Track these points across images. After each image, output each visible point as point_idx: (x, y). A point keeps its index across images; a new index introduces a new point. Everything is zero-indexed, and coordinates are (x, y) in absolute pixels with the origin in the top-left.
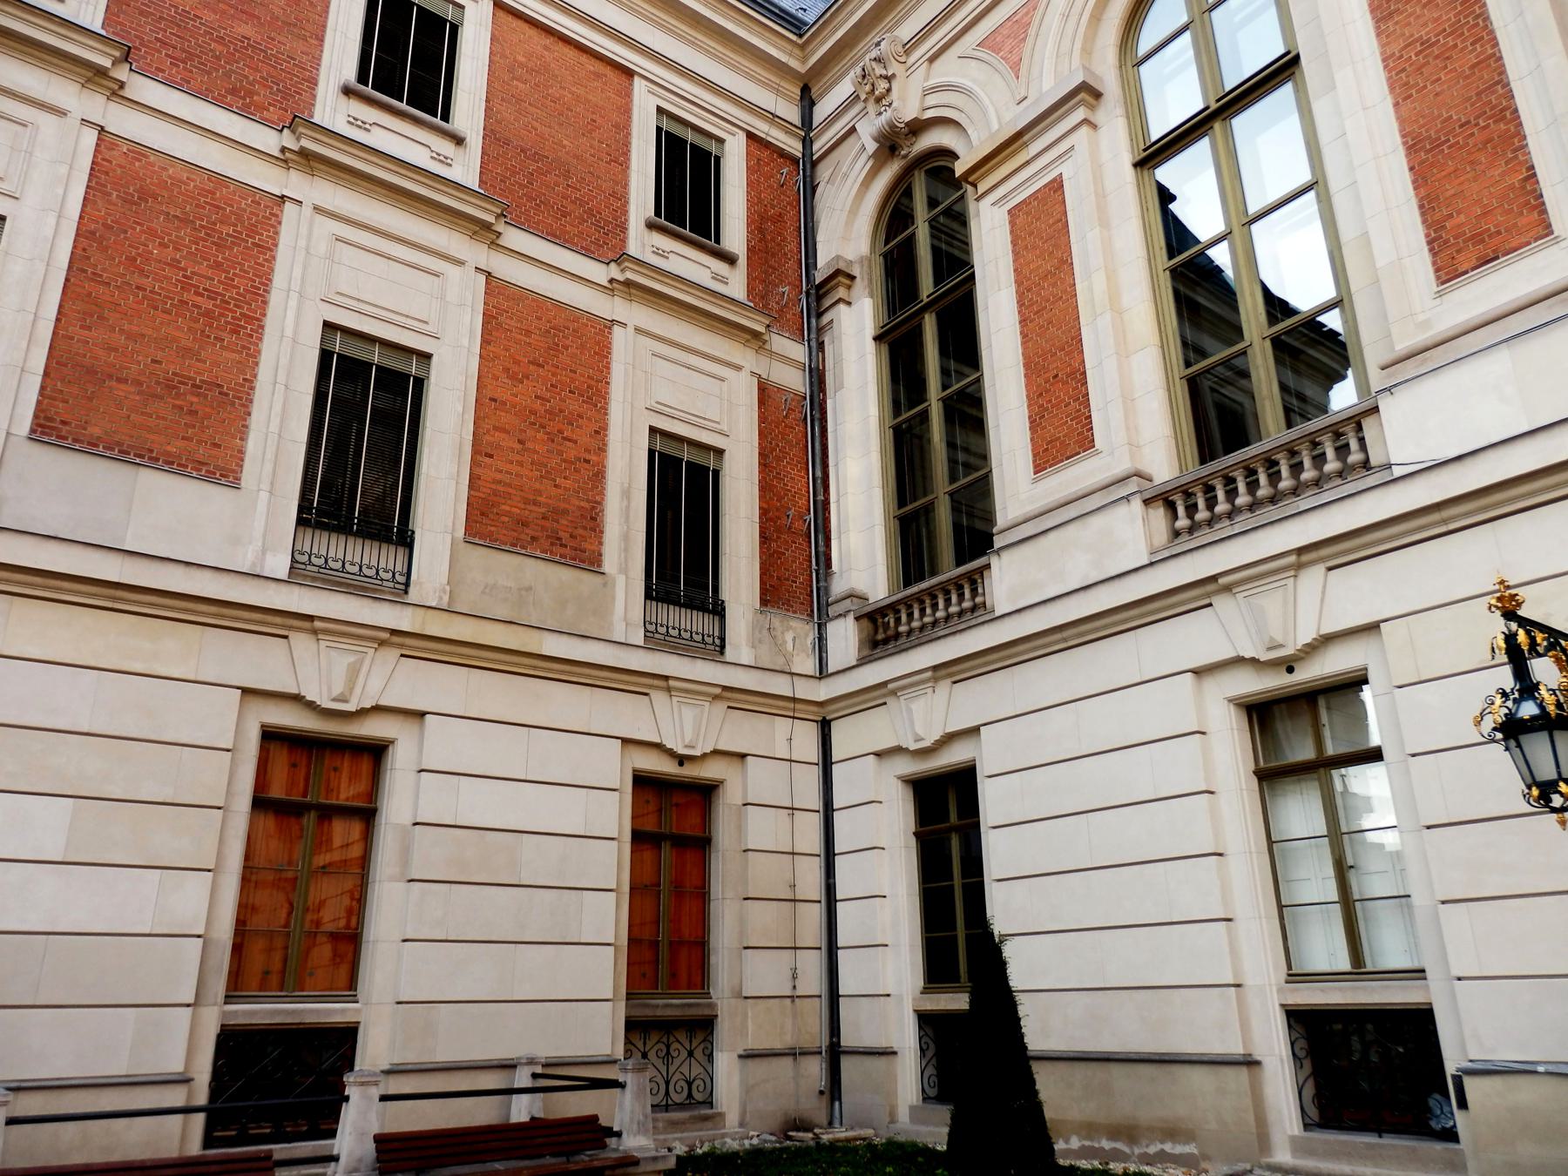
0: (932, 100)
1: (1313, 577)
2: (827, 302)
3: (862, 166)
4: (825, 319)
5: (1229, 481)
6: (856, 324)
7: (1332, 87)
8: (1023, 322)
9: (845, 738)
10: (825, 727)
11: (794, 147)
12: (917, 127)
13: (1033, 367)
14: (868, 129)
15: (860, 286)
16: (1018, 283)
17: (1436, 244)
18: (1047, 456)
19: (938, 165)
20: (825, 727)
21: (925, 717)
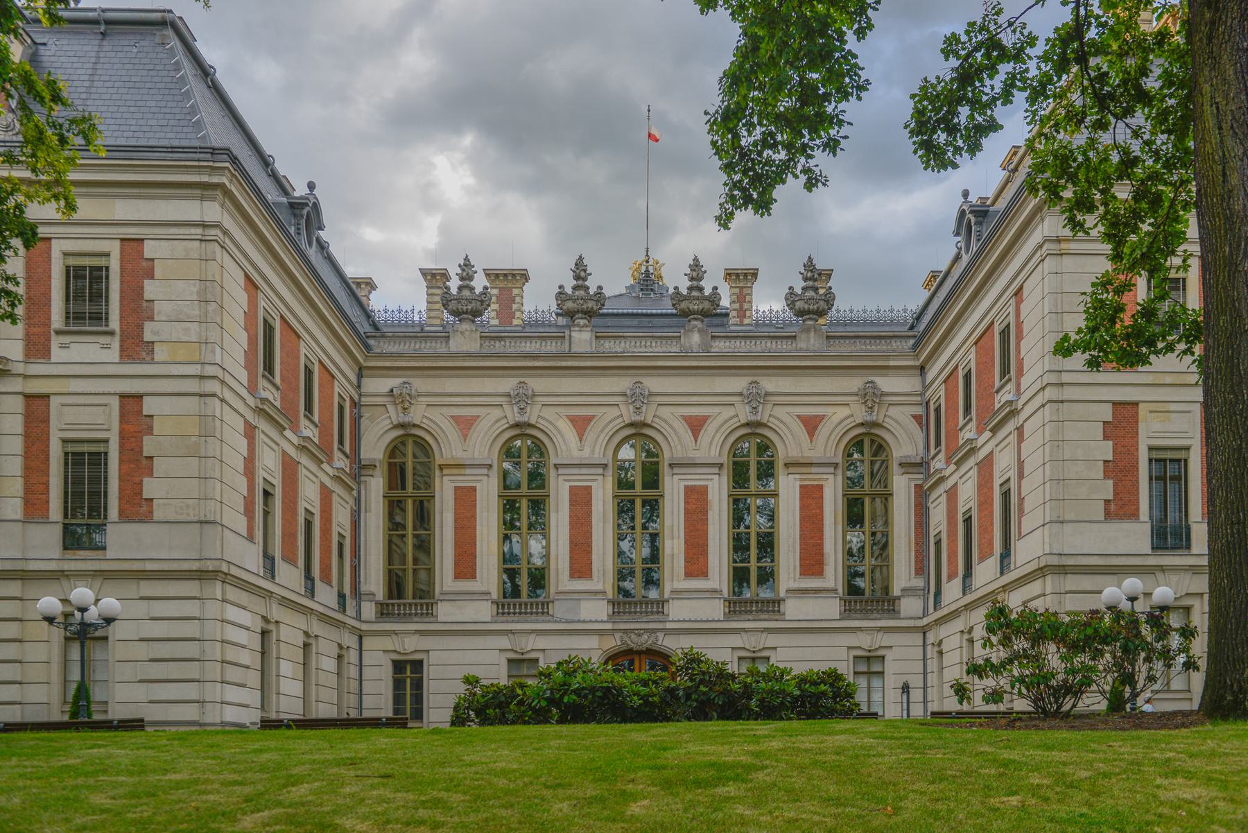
0: (425, 420)
1: (532, 636)
2: (363, 472)
3: (386, 424)
4: (363, 479)
5: (515, 605)
6: (376, 486)
7: (557, 511)
8: (456, 528)
9: (367, 642)
10: (361, 637)
11: (356, 397)
12: (415, 426)
13: (458, 545)
14: (395, 415)
15: (378, 472)
16: (456, 514)
17: (571, 568)
18: (458, 575)
19: (423, 447)
20: (361, 637)
21: (410, 646)
